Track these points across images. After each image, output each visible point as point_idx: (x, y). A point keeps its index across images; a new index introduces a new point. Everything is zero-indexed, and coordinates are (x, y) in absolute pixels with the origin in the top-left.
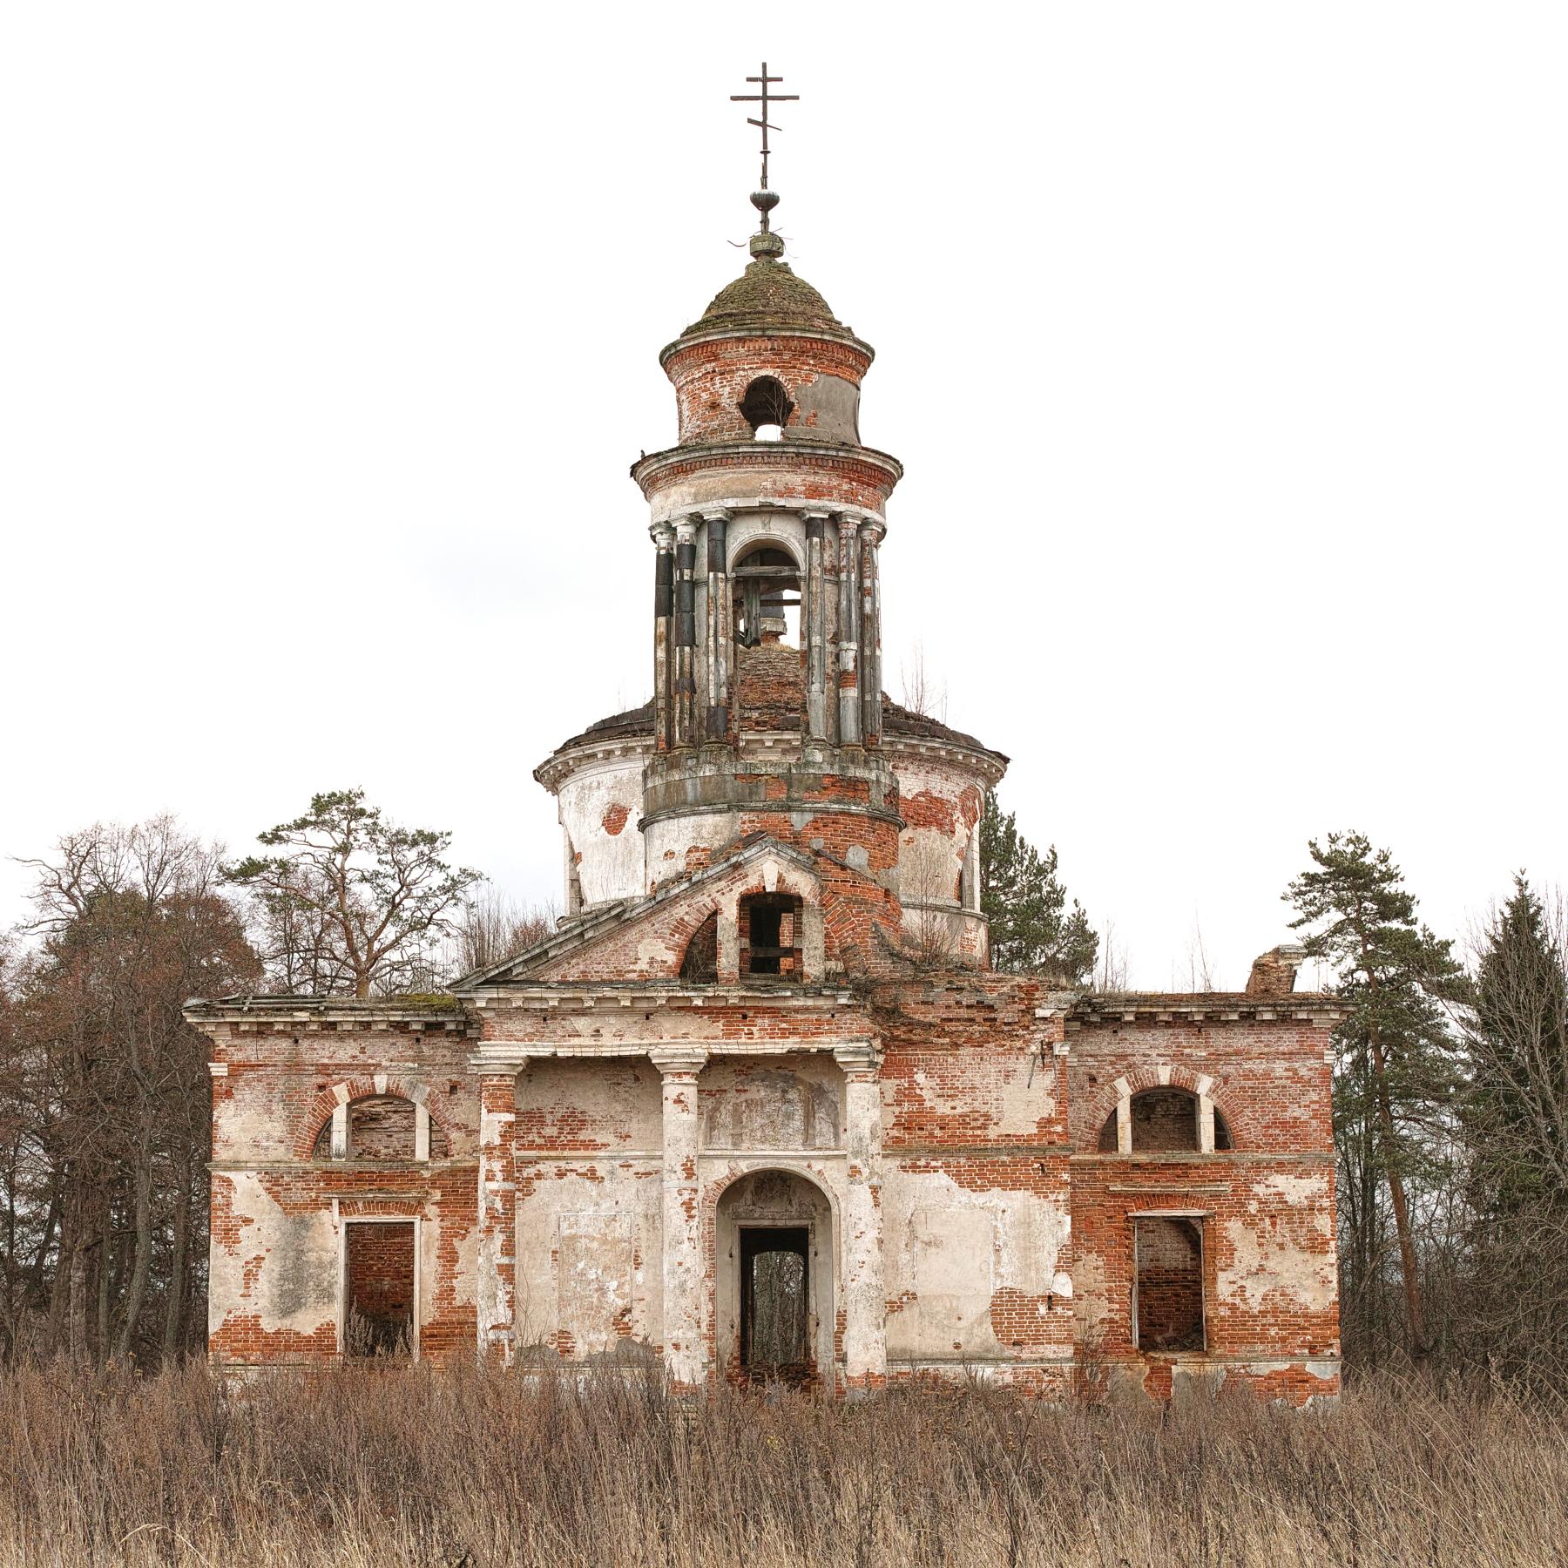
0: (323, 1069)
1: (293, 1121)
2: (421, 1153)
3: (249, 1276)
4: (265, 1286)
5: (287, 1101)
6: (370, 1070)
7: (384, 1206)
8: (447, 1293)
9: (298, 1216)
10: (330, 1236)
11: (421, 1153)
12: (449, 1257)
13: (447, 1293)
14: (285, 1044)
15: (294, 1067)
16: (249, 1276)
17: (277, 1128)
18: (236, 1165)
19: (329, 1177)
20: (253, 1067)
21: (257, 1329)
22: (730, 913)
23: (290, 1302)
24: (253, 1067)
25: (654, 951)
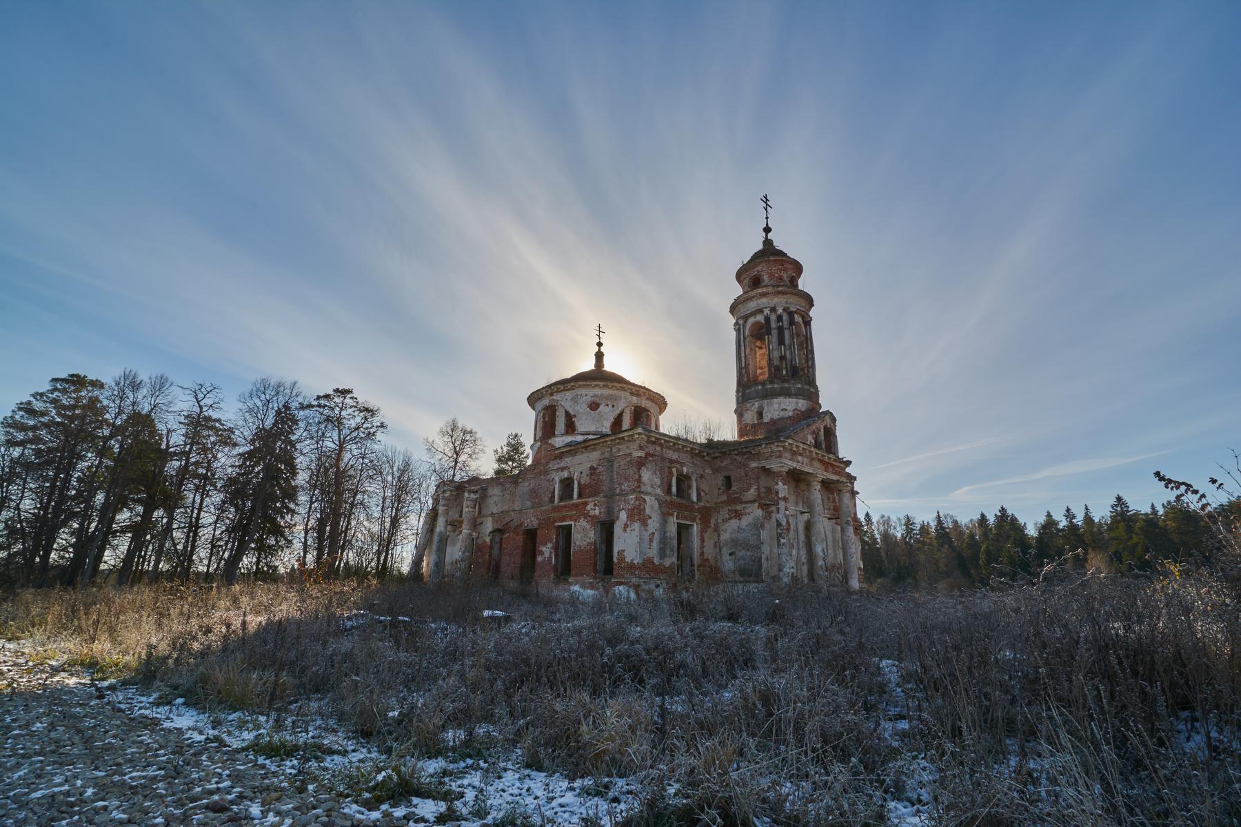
0: (671, 461)
1: (662, 479)
2: (695, 498)
3: (651, 540)
4: (655, 544)
5: (661, 471)
6: (682, 464)
7: (686, 518)
8: (702, 553)
9: (665, 516)
10: (672, 529)
11: (695, 498)
12: (702, 540)
13: (702, 553)
14: (658, 448)
15: (663, 459)
16: (651, 540)
17: (658, 481)
18: (648, 494)
19: (671, 503)
20: (652, 456)
21: (653, 563)
22: (822, 432)
23: (662, 553)
24: (652, 456)
25: (810, 439)
